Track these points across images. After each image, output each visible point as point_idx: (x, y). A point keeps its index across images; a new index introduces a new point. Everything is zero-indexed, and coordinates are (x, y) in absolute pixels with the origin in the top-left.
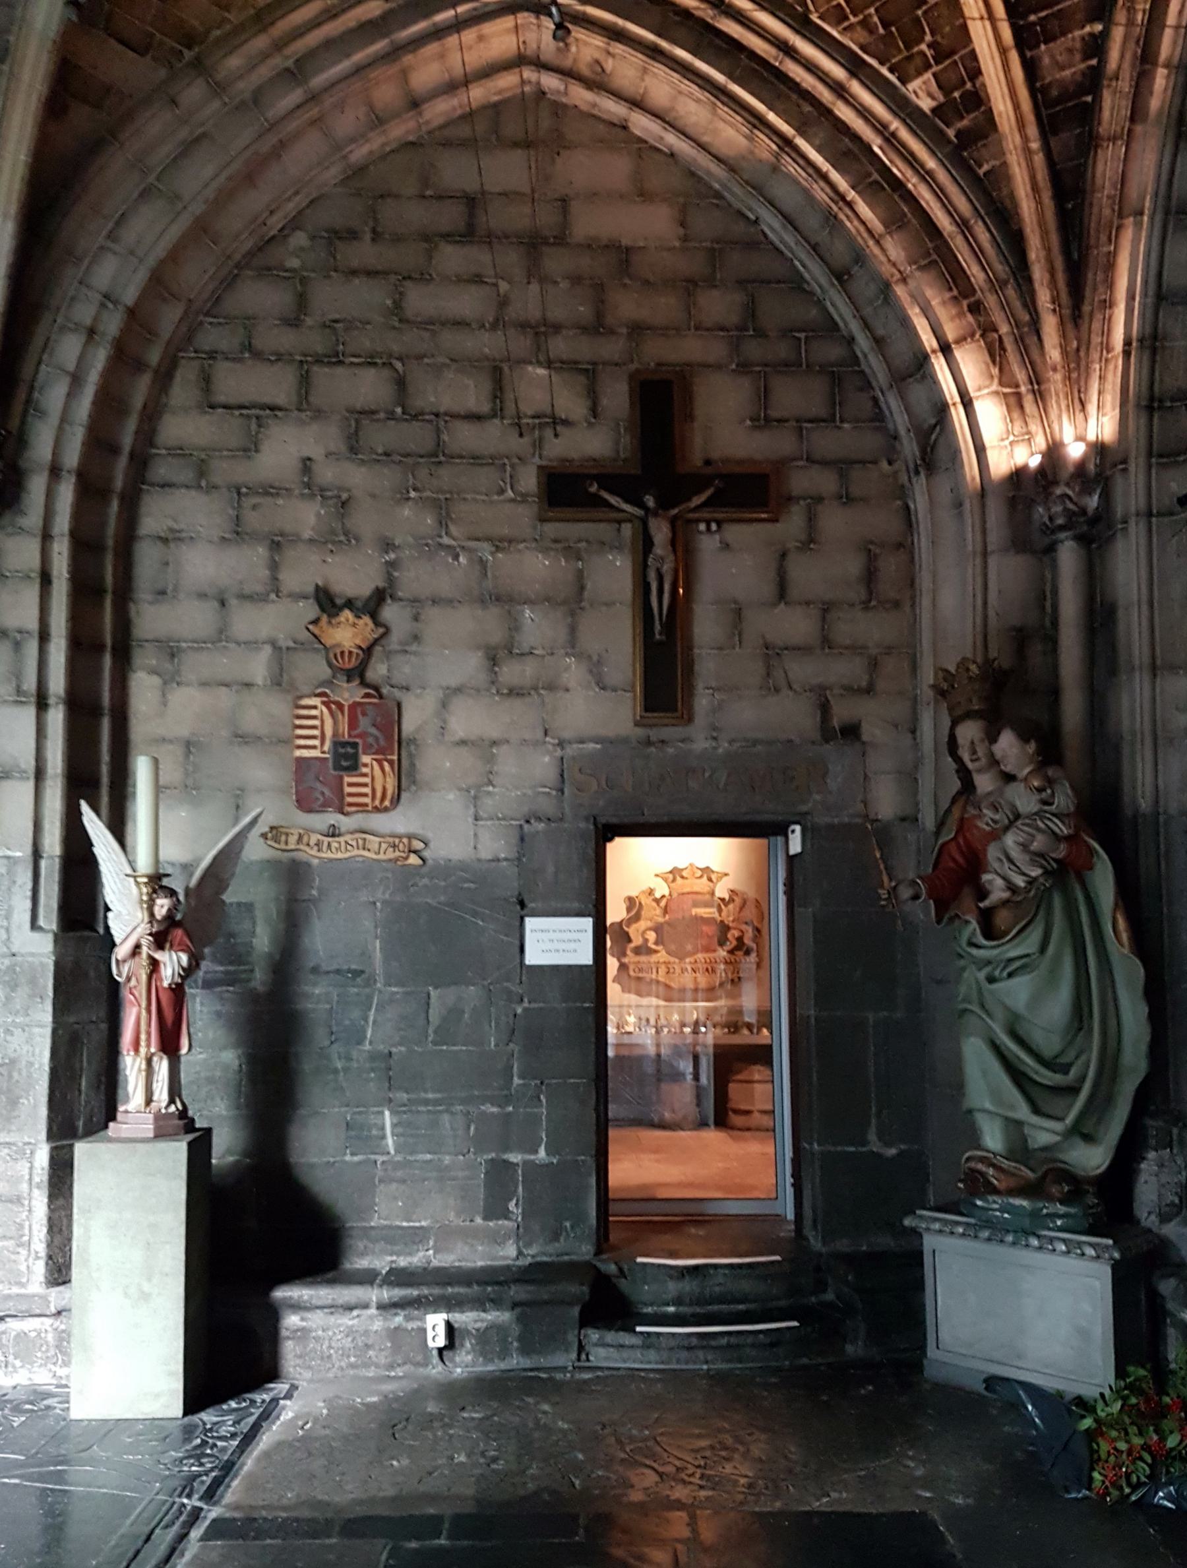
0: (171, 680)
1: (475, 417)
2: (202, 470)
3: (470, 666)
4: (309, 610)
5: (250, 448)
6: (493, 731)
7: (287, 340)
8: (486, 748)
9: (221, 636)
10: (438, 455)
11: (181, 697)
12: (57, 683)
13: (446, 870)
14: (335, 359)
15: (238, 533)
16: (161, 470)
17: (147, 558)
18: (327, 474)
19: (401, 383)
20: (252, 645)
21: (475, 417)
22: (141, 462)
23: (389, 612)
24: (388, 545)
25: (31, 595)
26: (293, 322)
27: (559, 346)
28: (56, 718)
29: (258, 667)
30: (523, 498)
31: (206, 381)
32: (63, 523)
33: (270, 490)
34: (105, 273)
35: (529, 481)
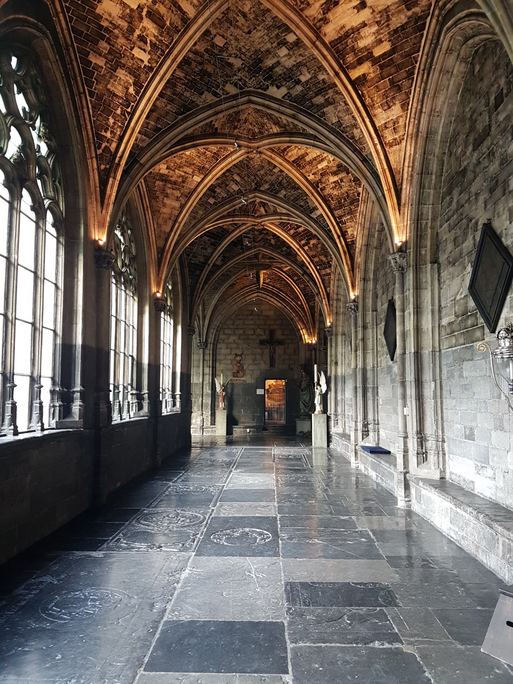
0: (220, 364)
1: (252, 335)
2: (224, 341)
3: (251, 362)
4: (235, 356)
5: (228, 338)
6: (253, 369)
7: (232, 327)
8: (253, 370)
9: (225, 359)
10: (248, 339)
11: (221, 365)
12: (211, 365)
13: (249, 384)
14: (237, 329)
15: (227, 348)
16: (219, 341)
17: (218, 350)
18: (236, 341)
19: (244, 331)
20: (229, 360)
21: (252, 335)
22: (217, 340)
23: (243, 356)
24: (243, 349)
25: (208, 356)
26: (233, 325)
27: (261, 327)
28: (211, 368)
29: (229, 362)
30: (257, 343)
31: (224, 332)
32: (211, 349)
33: (231, 343)
34: (215, 323)
35: (258, 341)
